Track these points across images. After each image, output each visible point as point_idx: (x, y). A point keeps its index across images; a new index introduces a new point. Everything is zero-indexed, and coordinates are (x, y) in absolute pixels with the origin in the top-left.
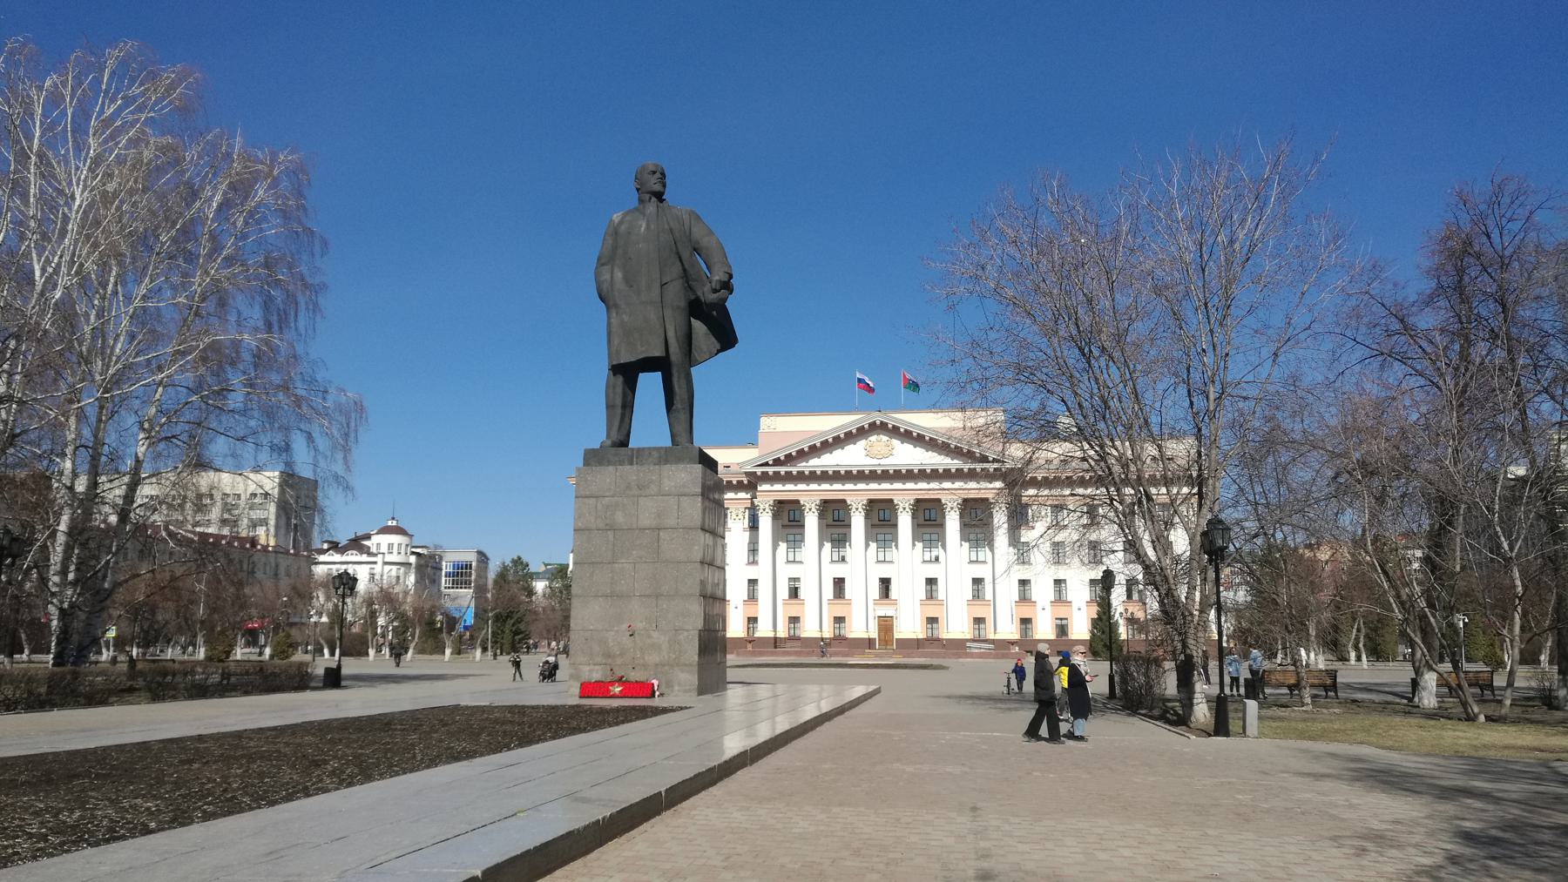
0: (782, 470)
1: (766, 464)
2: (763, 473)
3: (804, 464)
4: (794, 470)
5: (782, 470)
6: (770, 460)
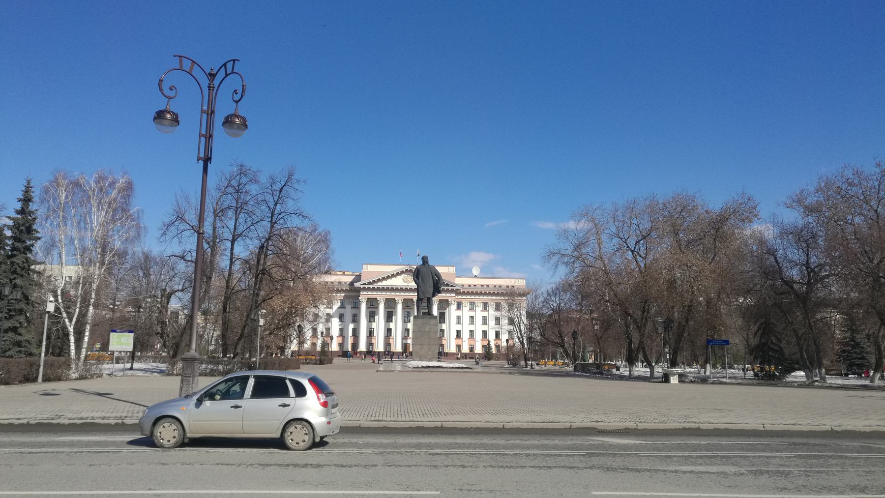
5: (371, 287)
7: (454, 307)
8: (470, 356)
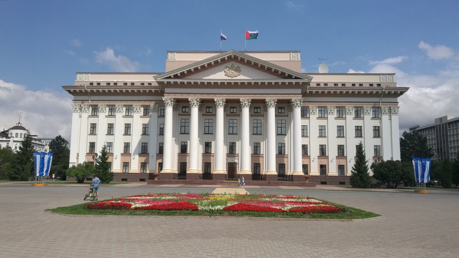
1: (170, 77)
2: (168, 82)
4: (185, 81)
5: (179, 81)
6: (172, 75)
7: (298, 111)
8: (323, 180)
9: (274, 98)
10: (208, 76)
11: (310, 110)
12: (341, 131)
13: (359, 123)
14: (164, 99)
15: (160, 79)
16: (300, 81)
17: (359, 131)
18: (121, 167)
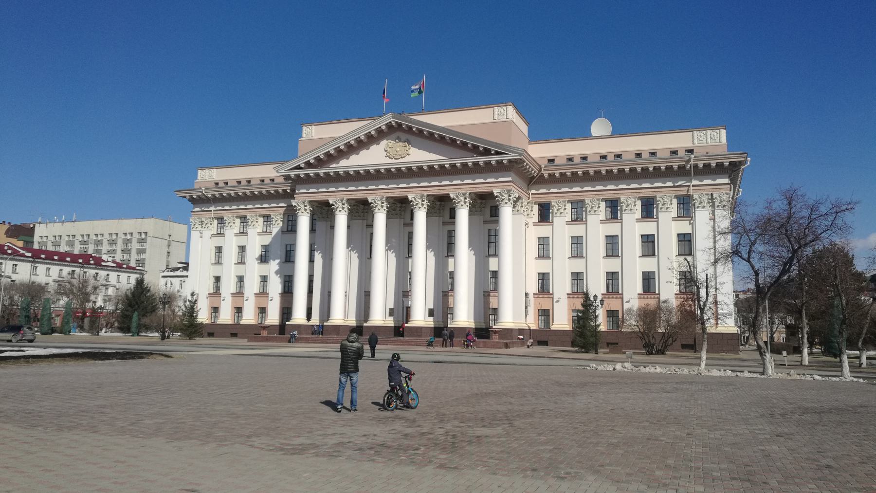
0: (311, 172)
1: (298, 168)
3: (334, 165)
4: (321, 171)
5: (311, 172)
9: (465, 190)
10: (430, 153)
11: (554, 208)
12: (613, 246)
13: (649, 228)
14: (294, 203)
15: (283, 171)
16: (505, 159)
17: (649, 243)
18: (255, 315)
